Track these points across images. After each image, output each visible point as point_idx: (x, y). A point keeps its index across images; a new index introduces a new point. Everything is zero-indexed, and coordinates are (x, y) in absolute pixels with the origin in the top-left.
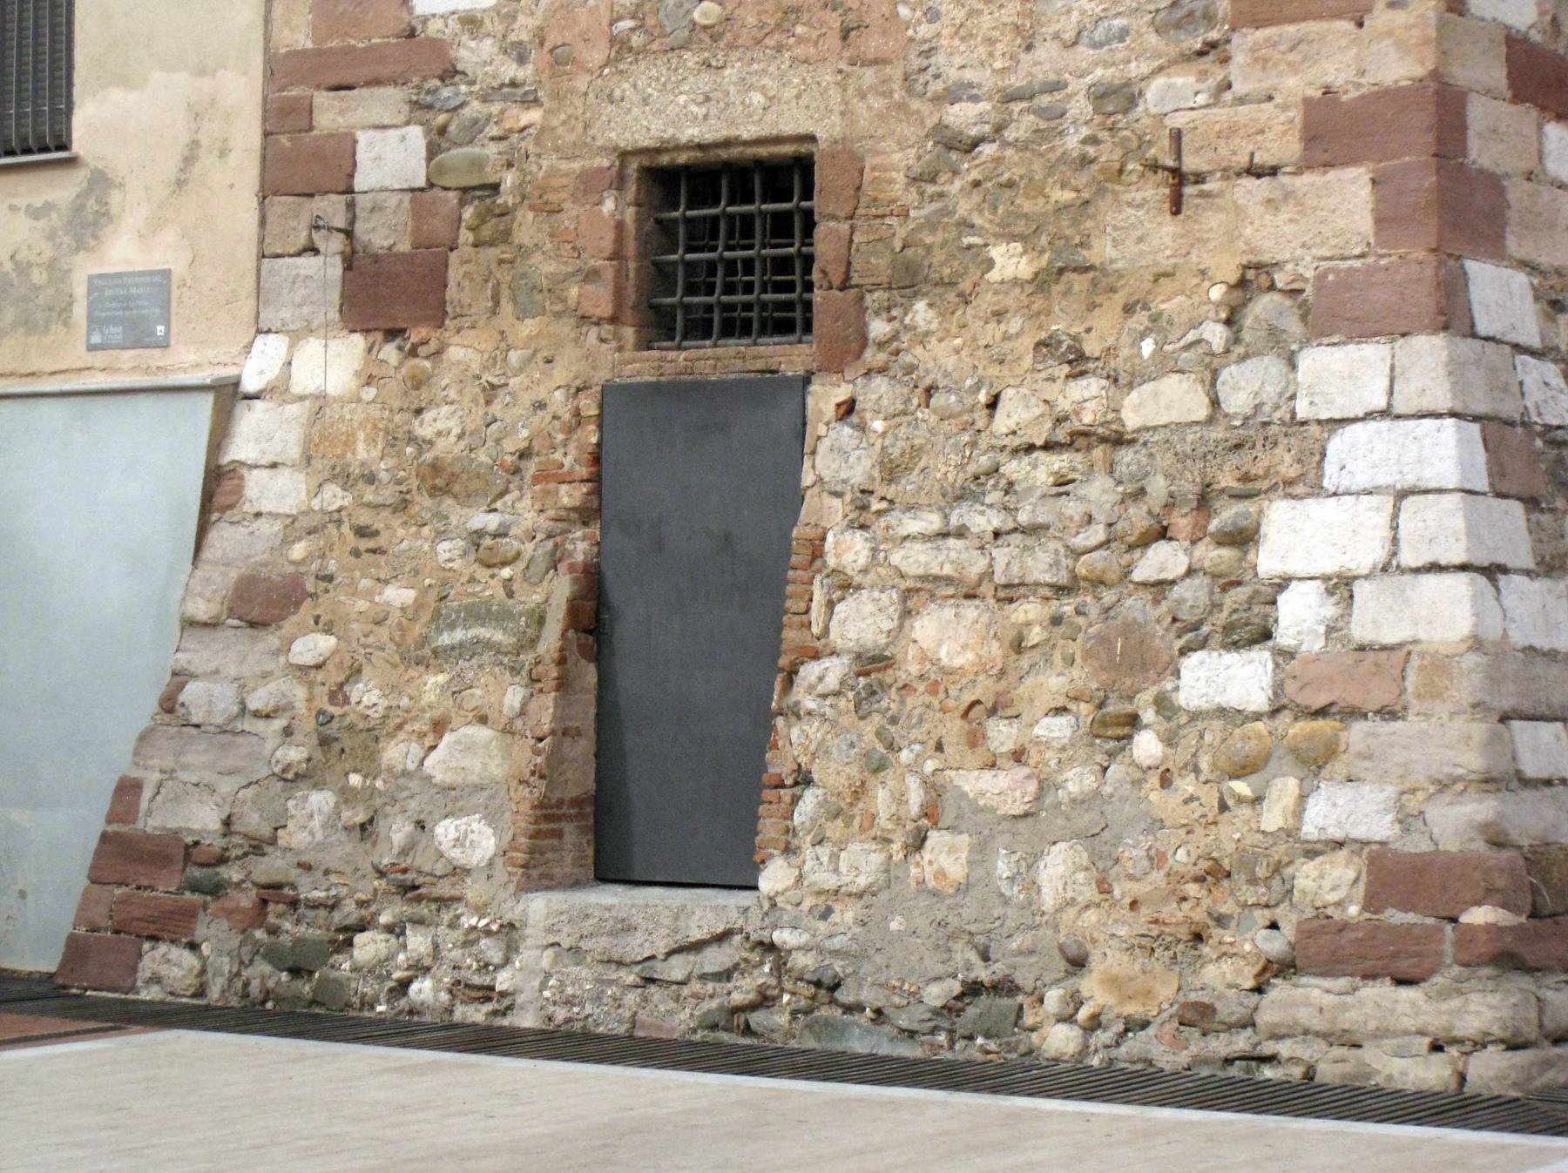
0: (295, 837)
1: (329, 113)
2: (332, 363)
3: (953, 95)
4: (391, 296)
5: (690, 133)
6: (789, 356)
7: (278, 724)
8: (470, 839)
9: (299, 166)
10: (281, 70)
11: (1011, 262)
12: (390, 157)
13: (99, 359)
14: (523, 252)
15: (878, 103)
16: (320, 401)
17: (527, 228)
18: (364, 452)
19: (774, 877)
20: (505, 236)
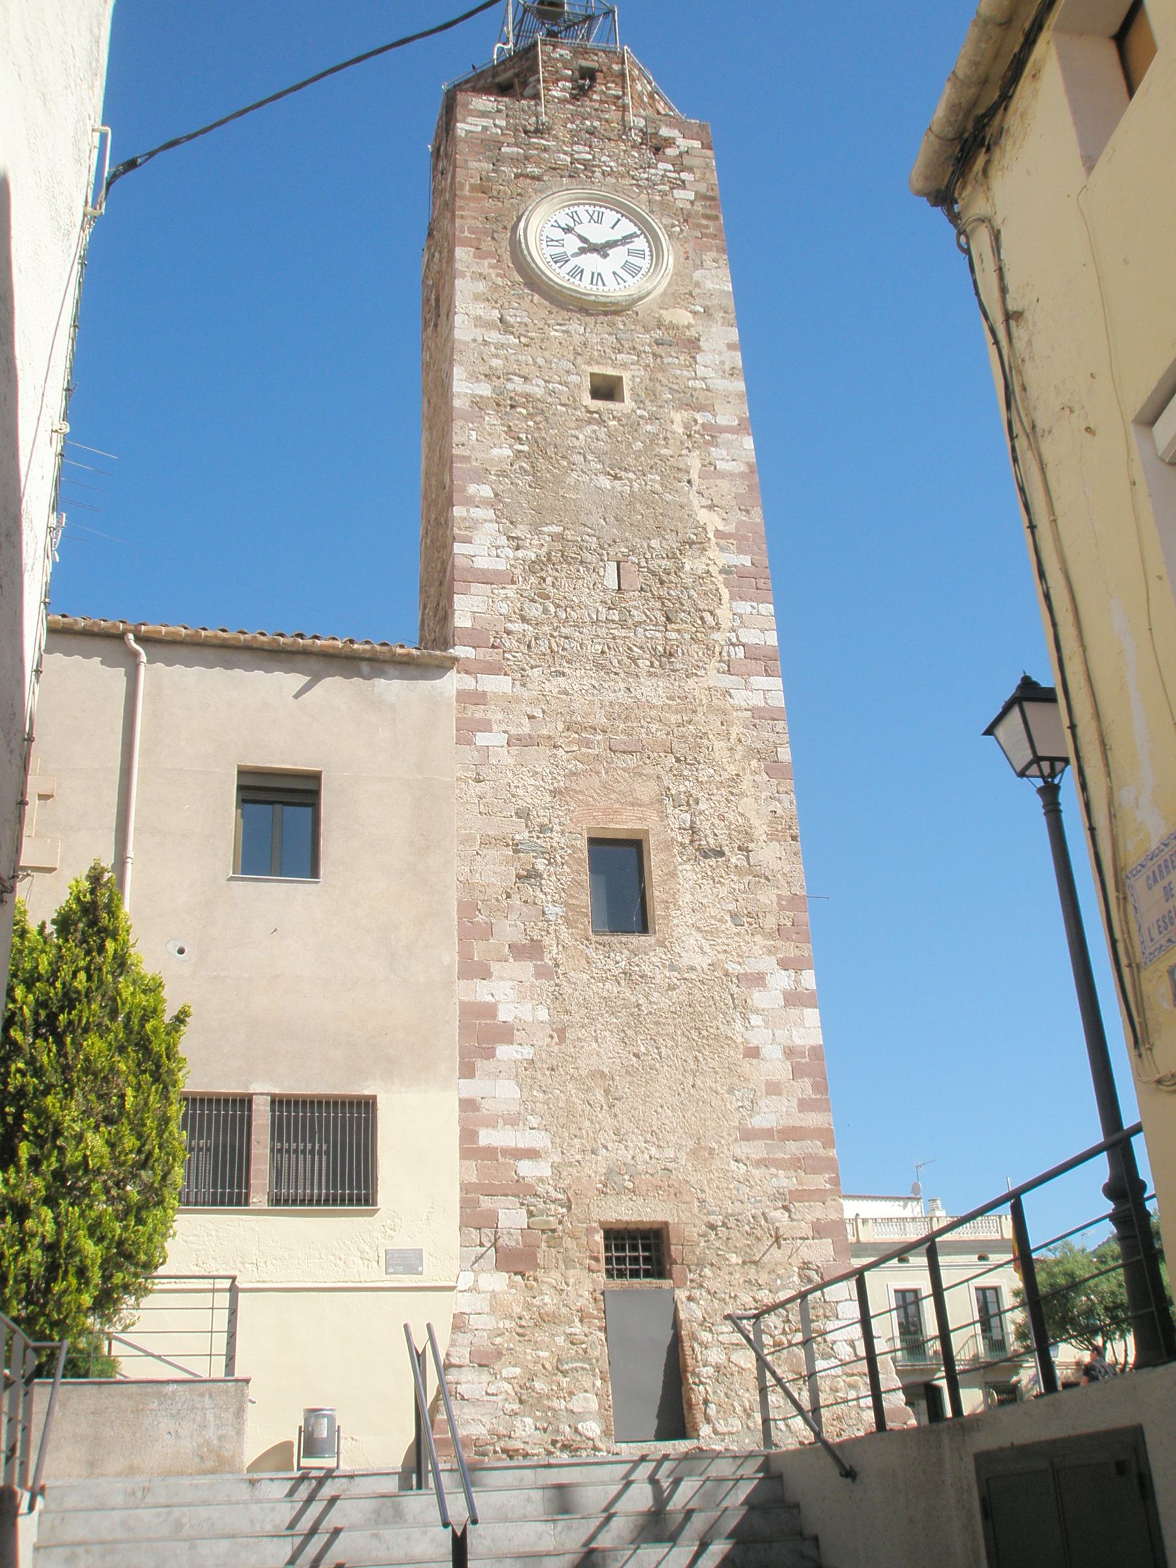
0: (519, 1433)
1: (486, 1203)
2: (497, 1281)
3: (709, 1213)
4: (517, 1261)
5: (626, 1218)
6: (666, 1284)
7: (499, 1397)
8: (592, 1428)
9: (474, 1218)
10: (466, 1188)
11: (734, 1259)
12: (512, 1218)
13: (388, 1277)
14: (566, 1250)
15: (688, 1214)
16: (494, 1294)
17: (568, 1242)
18: (518, 1310)
19: (705, 1430)
20: (560, 1245)
